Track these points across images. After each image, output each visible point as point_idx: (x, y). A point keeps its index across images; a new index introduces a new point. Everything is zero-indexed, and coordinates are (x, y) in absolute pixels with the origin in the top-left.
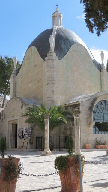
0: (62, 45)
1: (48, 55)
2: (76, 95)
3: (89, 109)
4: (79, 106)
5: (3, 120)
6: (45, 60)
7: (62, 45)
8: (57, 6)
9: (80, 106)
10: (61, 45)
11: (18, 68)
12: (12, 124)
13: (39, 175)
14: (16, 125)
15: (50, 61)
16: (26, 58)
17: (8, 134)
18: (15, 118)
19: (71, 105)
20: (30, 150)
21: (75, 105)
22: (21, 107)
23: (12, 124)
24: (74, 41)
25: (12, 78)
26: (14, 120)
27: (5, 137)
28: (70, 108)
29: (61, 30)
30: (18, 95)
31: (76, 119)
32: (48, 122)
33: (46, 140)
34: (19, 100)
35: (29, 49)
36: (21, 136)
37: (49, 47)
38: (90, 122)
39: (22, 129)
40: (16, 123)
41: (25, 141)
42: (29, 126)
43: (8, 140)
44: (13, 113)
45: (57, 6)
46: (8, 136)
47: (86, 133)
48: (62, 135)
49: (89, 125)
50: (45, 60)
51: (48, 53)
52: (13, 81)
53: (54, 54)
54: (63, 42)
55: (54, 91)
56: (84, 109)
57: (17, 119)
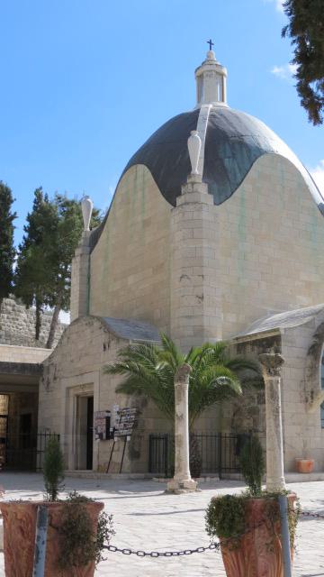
0: (227, 160)
1: (183, 190)
2: (271, 309)
3: (309, 354)
4: (279, 344)
5: (52, 385)
6: (174, 204)
7: (227, 160)
8: (210, 43)
9: (283, 343)
10: (222, 160)
11: (94, 229)
12: (78, 397)
13: (135, 555)
14: (90, 400)
15: (191, 207)
17: (66, 427)
18: (87, 379)
19: (254, 339)
20: (132, 476)
21: (266, 339)
22: (105, 347)
23: (78, 397)
24: (263, 147)
25: (78, 259)
28: (253, 350)
29: (221, 115)
30: (94, 310)
31: (271, 382)
32: (184, 392)
33: (180, 446)
34: (97, 324)
35: (130, 170)
36: (104, 435)
37: (187, 167)
38: (312, 392)
39: (108, 412)
40: (89, 395)
41: (116, 448)
42: (127, 402)
43: (66, 444)
44: (79, 365)
45: (210, 43)
46: (66, 433)
47: (300, 424)
48: (227, 432)
49: (310, 399)
50: (174, 204)
51: (185, 183)
52: (81, 269)
53: (202, 188)
54: (229, 153)
55: (202, 298)
56: (292, 353)
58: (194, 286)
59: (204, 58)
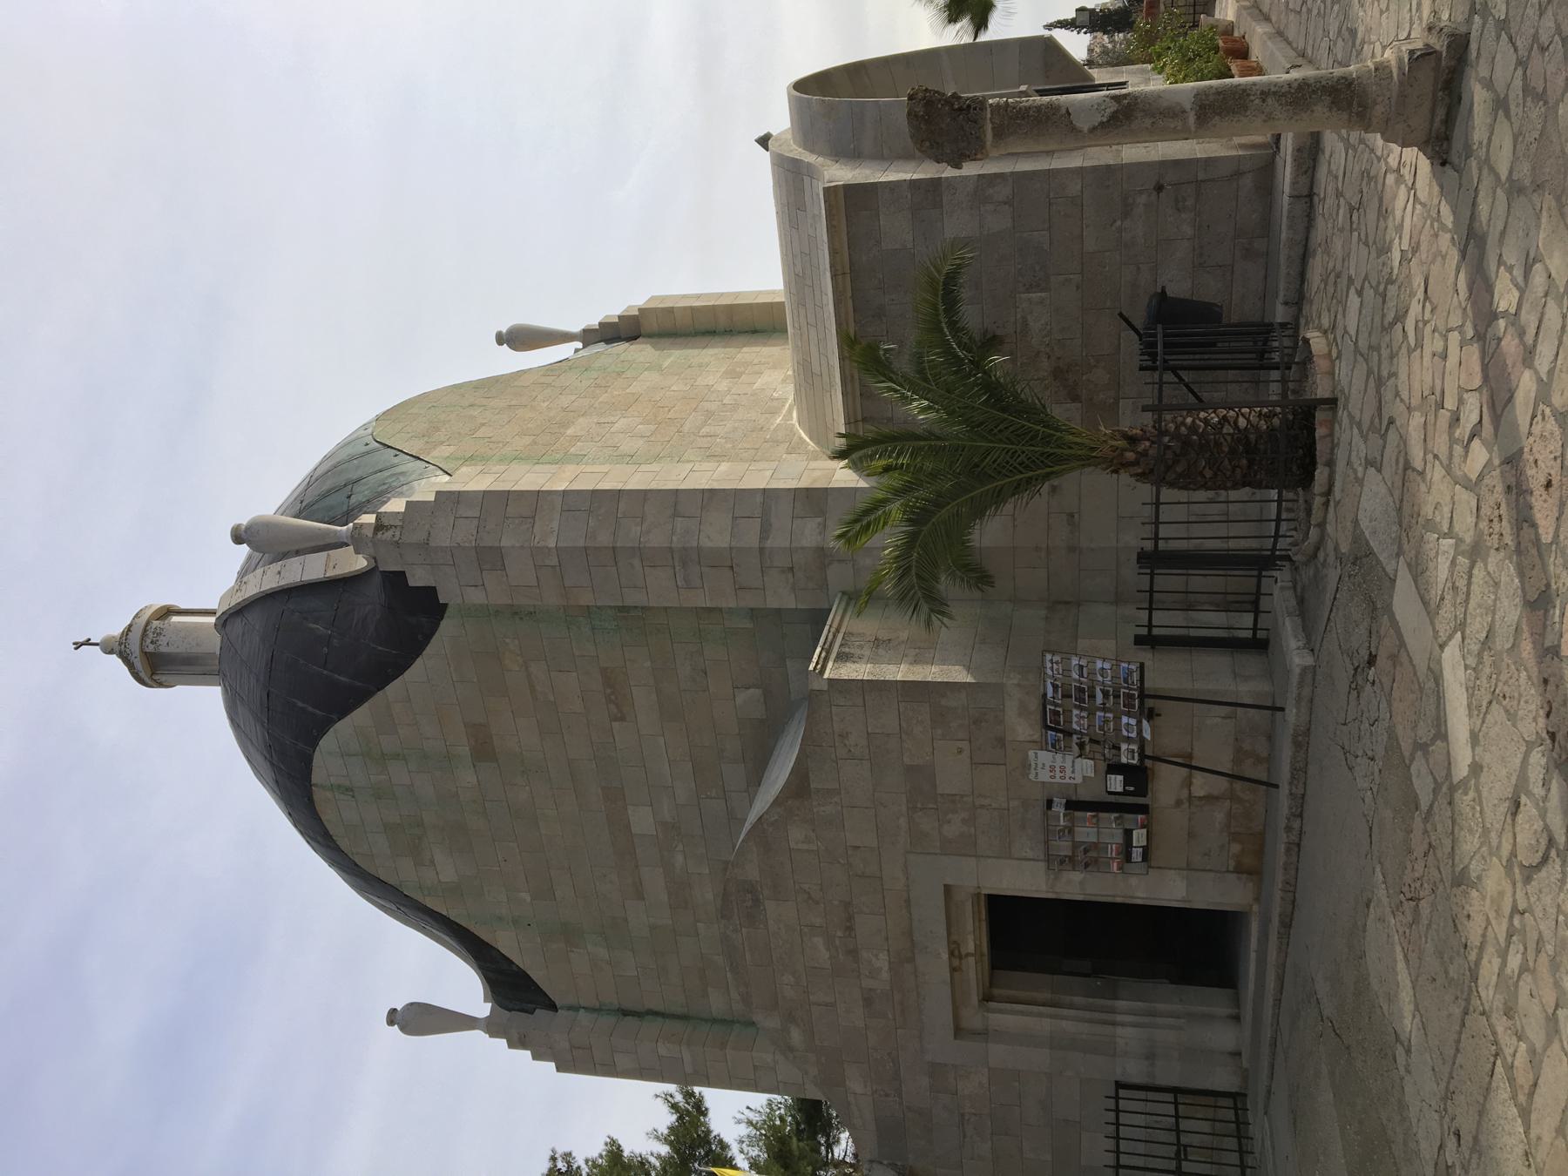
8: (78, 645)
12: (987, 998)
16: (404, 873)
23: (987, 998)
26: (955, 952)
27: (1122, 1093)
40: (974, 937)
44: (882, 962)
57: (948, 889)
58: (675, 515)
59: (115, 659)
